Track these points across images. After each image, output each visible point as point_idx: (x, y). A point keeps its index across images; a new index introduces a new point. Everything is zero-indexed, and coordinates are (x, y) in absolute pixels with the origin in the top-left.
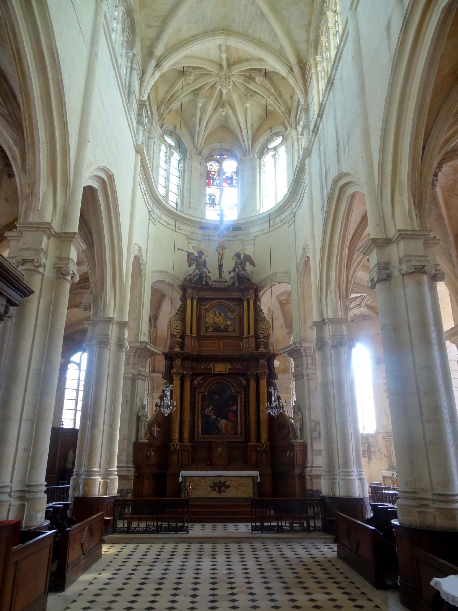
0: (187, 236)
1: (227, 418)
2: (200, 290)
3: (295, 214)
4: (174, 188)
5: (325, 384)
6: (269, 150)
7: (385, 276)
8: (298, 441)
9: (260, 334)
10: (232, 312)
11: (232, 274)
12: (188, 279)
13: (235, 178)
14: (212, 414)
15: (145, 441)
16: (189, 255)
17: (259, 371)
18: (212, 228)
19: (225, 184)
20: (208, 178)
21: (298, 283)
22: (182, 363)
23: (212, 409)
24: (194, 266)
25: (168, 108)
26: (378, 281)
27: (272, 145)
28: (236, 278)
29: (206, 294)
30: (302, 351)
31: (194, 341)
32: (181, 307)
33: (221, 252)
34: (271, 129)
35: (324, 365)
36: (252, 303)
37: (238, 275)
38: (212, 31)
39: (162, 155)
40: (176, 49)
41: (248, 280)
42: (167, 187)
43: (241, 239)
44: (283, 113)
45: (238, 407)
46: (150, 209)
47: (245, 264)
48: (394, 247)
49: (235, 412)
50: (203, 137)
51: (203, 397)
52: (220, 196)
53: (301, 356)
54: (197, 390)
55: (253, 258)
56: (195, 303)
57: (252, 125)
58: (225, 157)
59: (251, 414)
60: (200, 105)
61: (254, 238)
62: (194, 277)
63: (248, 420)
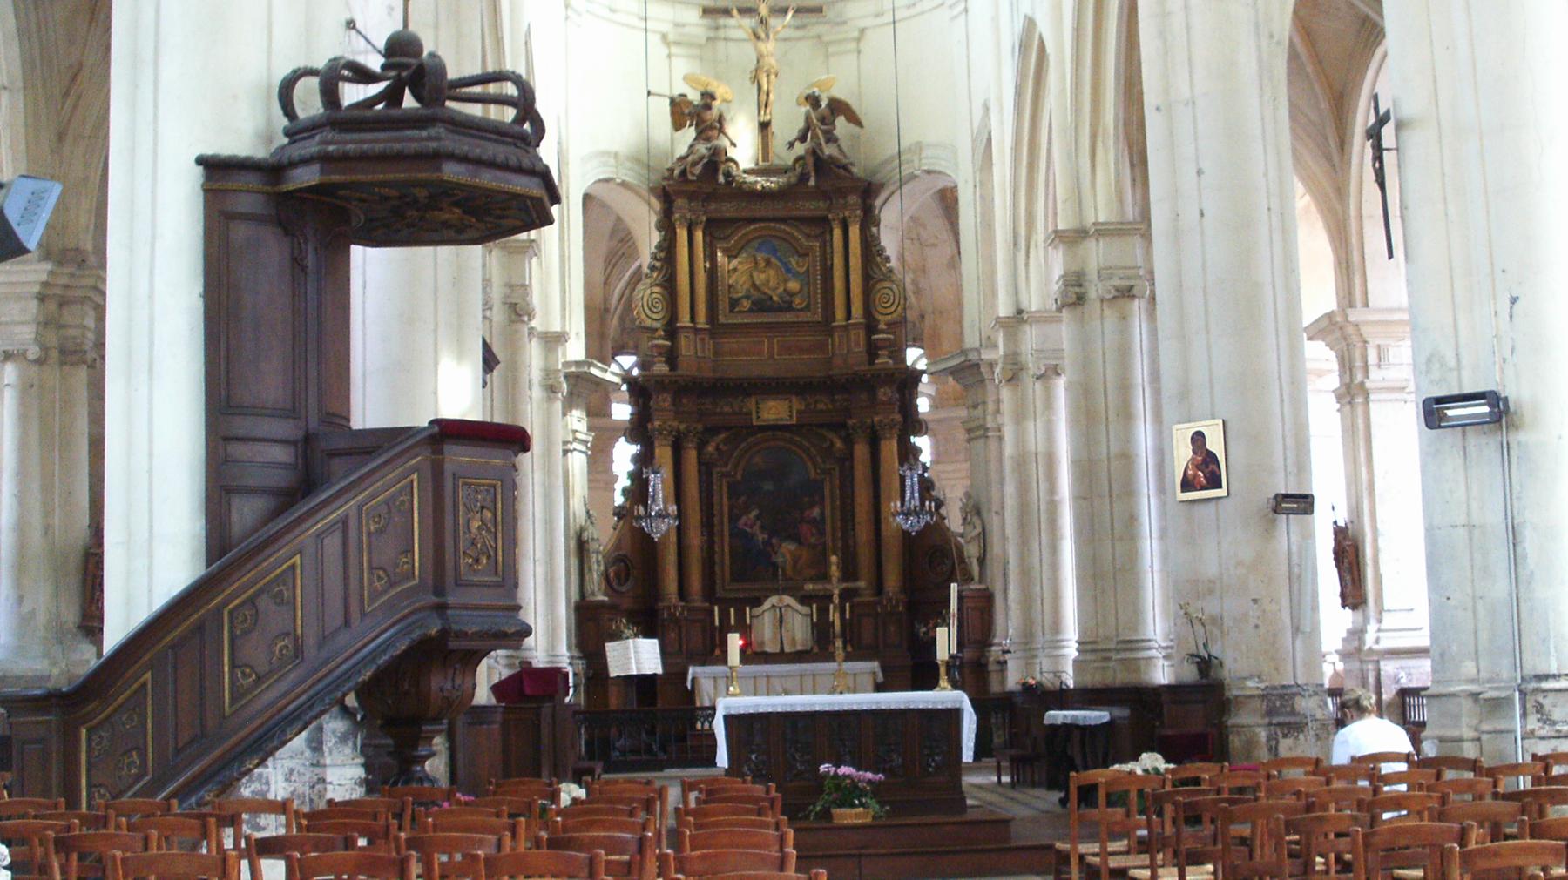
1: (796, 538)
2: (709, 198)
5: (1021, 462)
7: (1074, 299)
8: (972, 586)
9: (880, 317)
10: (800, 256)
11: (800, 149)
12: (677, 172)
14: (756, 529)
15: (601, 597)
17: (876, 419)
18: (735, 12)
22: (674, 404)
23: (757, 517)
24: (690, 133)
26: (1063, 306)
28: (810, 161)
29: (728, 210)
30: (983, 369)
31: (702, 340)
32: (659, 247)
33: (765, 87)
35: (1020, 417)
36: (854, 231)
37: (814, 152)
41: (845, 168)
43: (819, 37)
45: (825, 510)
48: (1091, 244)
49: (818, 524)
51: (730, 486)
53: (983, 381)
54: (715, 471)
55: (854, 106)
56: (699, 235)
59: (858, 527)
61: (856, 34)
62: (694, 164)
63: (851, 542)
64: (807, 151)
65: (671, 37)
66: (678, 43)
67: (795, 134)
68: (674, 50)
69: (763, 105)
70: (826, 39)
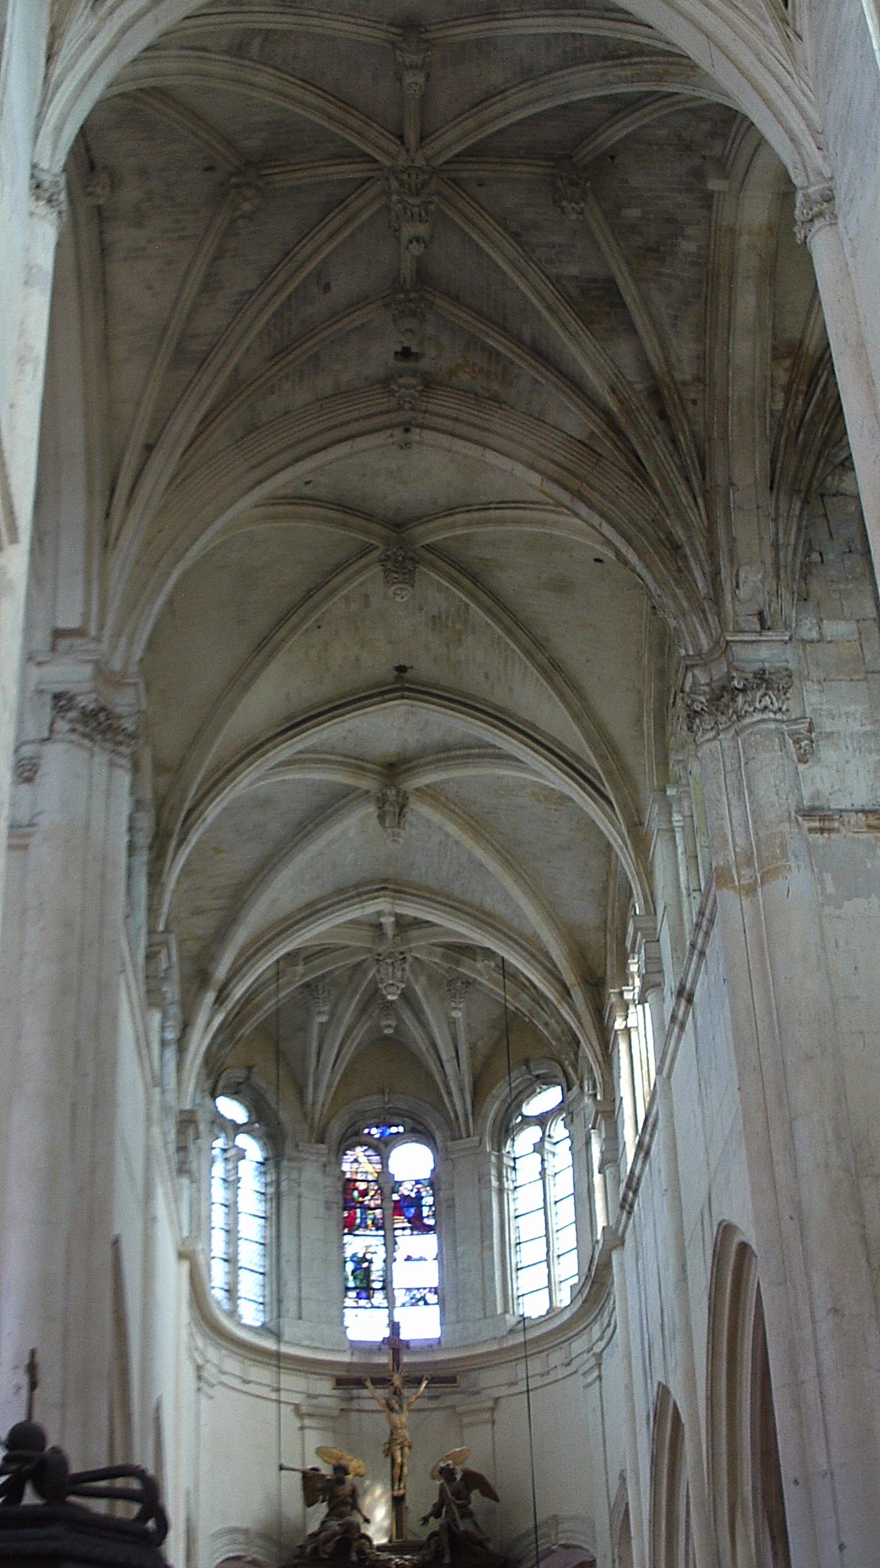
0: (297, 1408)
3: (599, 1356)
4: (251, 1255)
6: (527, 1121)
11: (434, 1524)
12: (308, 1550)
13: (428, 1200)
16: (310, 1479)
18: (368, 1384)
19: (401, 1222)
20: (349, 1204)
21: (614, 1561)
24: (321, 1509)
25: (231, 1037)
27: (534, 1107)
33: (399, 1460)
34: (526, 1062)
37: (449, 1528)
38: (356, 886)
39: (219, 1169)
40: (265, 945)
41: (480, 1543)
42: (231, 1260)
43: (453, 1407)
44: (558, 1039)
46: (200, 1362)
47: (467, 1497)
50: (329, 1087)
52: (389, 1261)
57: (472, 1048)
58: (394, 1130)
60: (324, 1019)
61: (490, 1404)
62: (327, 1541)
64: (441, 1526)
65: (304, 1409)
66: (310, 1415)
67: (429, 1509)
68: (307, 1422)
69: (397, 1479)
70: (460, 1409)
